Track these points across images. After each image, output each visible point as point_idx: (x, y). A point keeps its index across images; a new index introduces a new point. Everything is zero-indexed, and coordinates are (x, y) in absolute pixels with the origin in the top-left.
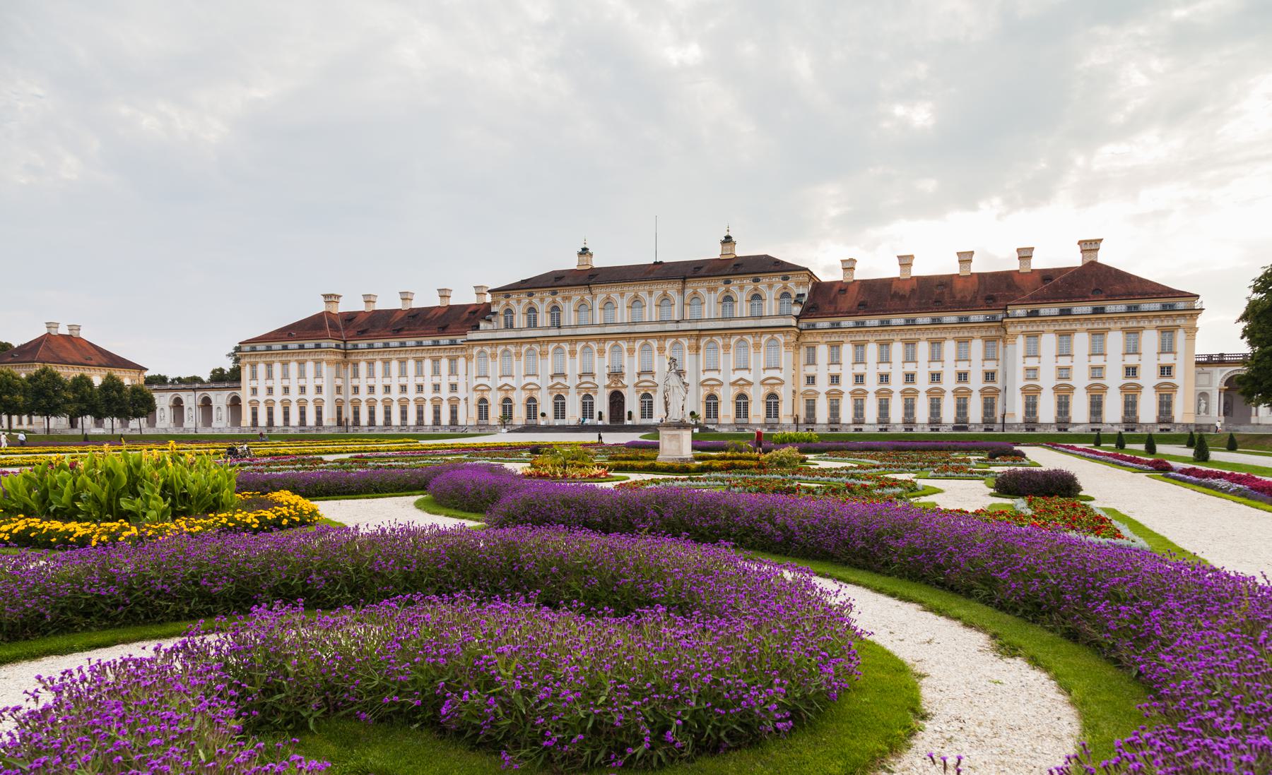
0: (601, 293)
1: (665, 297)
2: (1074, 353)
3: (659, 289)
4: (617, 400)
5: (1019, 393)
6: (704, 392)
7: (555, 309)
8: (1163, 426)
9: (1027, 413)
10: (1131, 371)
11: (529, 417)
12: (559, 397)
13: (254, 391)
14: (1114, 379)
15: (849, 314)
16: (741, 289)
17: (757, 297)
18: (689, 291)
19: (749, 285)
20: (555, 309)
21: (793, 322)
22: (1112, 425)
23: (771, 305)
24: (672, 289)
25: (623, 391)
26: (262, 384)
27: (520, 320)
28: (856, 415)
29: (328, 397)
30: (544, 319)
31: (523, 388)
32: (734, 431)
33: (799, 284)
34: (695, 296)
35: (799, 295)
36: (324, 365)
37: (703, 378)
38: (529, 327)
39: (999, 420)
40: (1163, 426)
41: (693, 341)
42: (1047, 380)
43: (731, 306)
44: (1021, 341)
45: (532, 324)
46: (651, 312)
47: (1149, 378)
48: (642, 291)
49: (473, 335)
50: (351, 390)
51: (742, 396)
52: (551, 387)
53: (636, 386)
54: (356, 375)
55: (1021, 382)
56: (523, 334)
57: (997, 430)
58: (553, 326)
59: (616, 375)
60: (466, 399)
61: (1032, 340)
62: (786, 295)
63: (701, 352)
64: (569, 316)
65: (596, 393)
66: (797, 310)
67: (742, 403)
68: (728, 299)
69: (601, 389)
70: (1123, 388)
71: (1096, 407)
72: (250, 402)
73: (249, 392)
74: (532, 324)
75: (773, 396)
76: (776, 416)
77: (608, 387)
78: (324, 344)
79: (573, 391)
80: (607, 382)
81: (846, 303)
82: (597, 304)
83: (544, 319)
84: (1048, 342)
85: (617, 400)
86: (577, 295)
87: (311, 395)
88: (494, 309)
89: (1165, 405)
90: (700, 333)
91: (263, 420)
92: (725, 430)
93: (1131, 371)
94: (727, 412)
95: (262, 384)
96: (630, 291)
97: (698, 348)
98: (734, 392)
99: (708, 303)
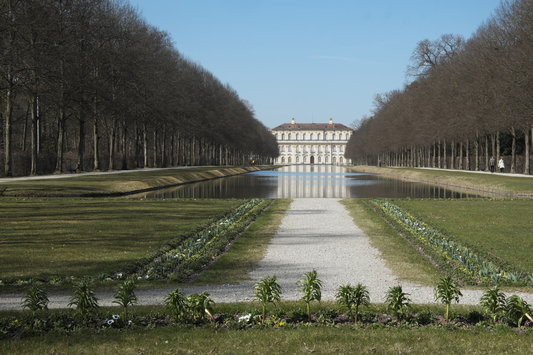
1: (319, 134)
3: (318, 132)
4: (312, 158)
6: (333, 156)
16: (337, 133)
19: (340, 132)
24: (322, 133)
30: (286, 137)
34: (326, 134)
38: (282, 140)
46: (315, 137)
59: (312, 152)
79: (301, 156)
83: (286, 137)
85: (312, 158)
96: (311, 132)
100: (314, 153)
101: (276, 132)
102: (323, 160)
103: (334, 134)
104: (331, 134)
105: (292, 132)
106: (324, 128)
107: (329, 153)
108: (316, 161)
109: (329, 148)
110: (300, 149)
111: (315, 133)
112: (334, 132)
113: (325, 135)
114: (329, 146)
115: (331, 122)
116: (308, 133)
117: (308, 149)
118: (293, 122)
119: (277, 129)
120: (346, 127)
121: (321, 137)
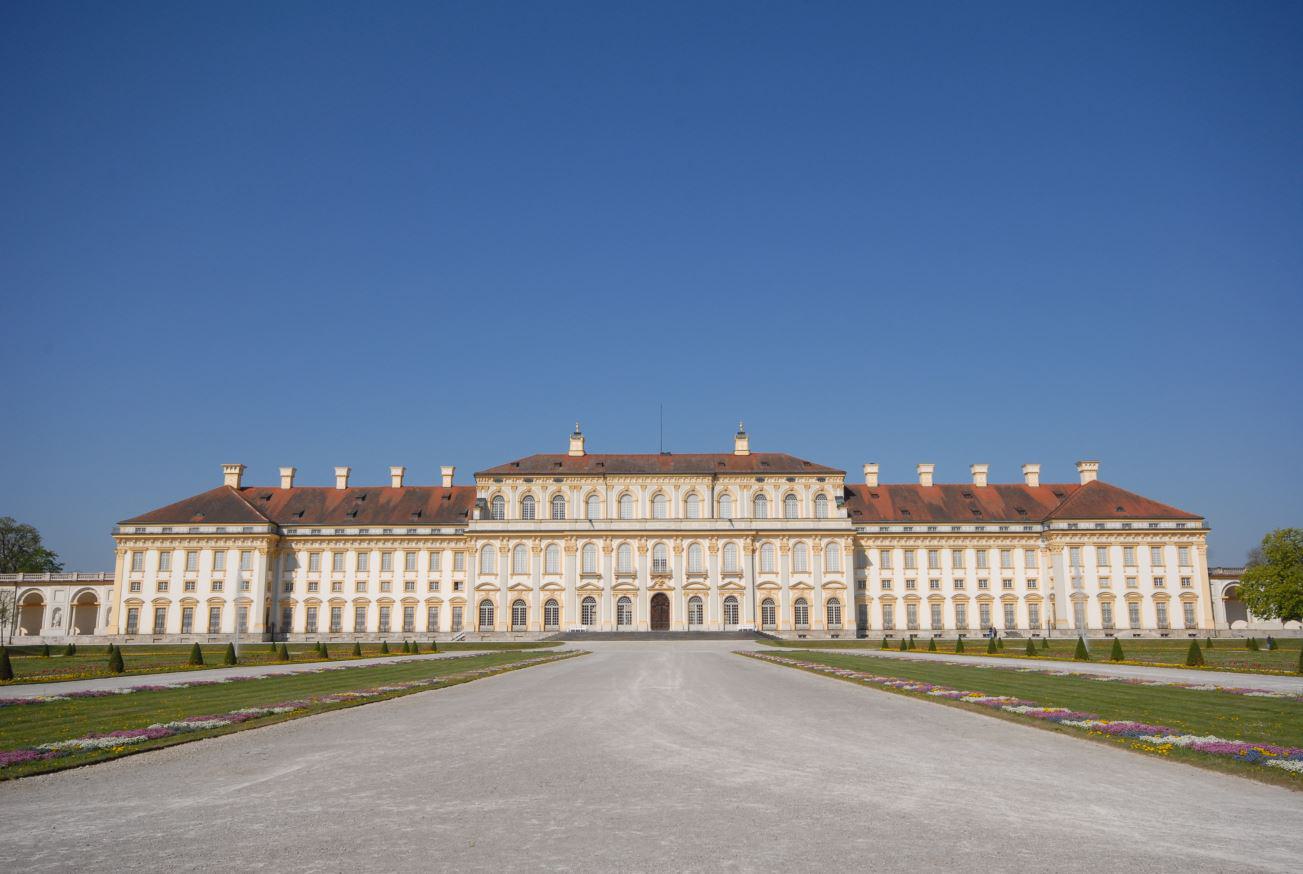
0: (619, 483)
1: (692, 493)
2: (1167, 563)
3: (687, 483)
4: (660, 606)
5: (1068, 599)
6: (760, 595)
7: (557, 498)
8: (1191, 632)
9: (1077, 619)
10: (1158, 581)
11: (547, 622)
12: (626, 599)
13: (135, 586)
14: (1146, 588)
15: (896, 522)
16: (775, 488)
17: (790, 497)
18: (719, 488)
20: (557, 498)
21: (848, 524)
22: (1150, 630)
23: (805, 507)
24: (702, 485)
25: (668, 593)
26: (150, 578)
27: (512, 510)
28: (909, 621)
29: (257, 594)
30: (543, 510)
31: (543, 588)
32: (794, 637)
33: (835, 487)
34: (725, 493)
35: (837, 498)
36: (257, 553)
37: (759, 580)
39: (1044, 626)
40: (1191, 632)
41: (749, 541)
42: (1091, 588)
43: (765, 505)
44: (1066, 550)
45: (527, 513)
47: (1173, 587)
48: (668, 485)
49: (472, 526)
50: (281, 588)
51: (800, 600)
52: (582, 588)
53: (685, 587)
54: (292, 565)
55: (1069, 590)
56: (543, 527)
57: (1044, 634)
58: (554, 517)
60: (1052, 597)
61: (957, 554)
62: (820, 496)
63: (757, 553)
64: (575, 507)
65: (636, 595)
66: (844, 512)
67: (801, 611)
68: (759, 497)
69: (643, 589)
70: (1181, 596)
71: (1134, 613)
72: (127, 601)
73: (126, 587)
74: (527, 513)
75: (833, 600)
76: (838, 621)
77: (652, 588)
78: (259, 528)
79: (608, 591)
80: (650, 583)
81: (884, 504)
82: (648, 495)
83: (543, 510)
84: (1089, 553)
85: (660, 606)
86: (587, 484)
87: (230, 592)
88: (481, 495)
89: (1189, 613)
90: (756, 535)
91: (146, 625)
92: (785, 637)
93: (1158, 581)
94: (784, 620)
95: (150, 578)
96: (653, 483)
97: (754, 551)
98: (793, 595)
99: (738, 497)
100: (670, 577)
101: (493, 486)
102: (714, 619)
103: (759, 497)
104: (747, 495)
105: (565, 486)
106: (717, 467)
107: (740, 576)
108: (678, 620)
109: (742, 561)
110: (602, 559)
111: (674, 490)
112: (756, 486)
113: (716, 501)
114: (740, 543)
115: (742, 447)
116: (640, 489)
117: (638, 559)
118: (576, 448)
119: (498, 475)
120: (806, 463)
121: (704, 510)
